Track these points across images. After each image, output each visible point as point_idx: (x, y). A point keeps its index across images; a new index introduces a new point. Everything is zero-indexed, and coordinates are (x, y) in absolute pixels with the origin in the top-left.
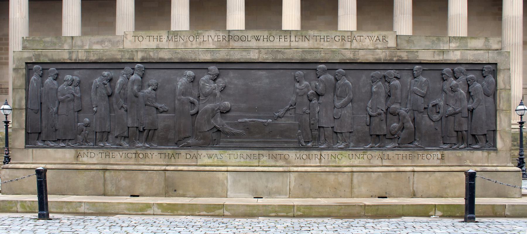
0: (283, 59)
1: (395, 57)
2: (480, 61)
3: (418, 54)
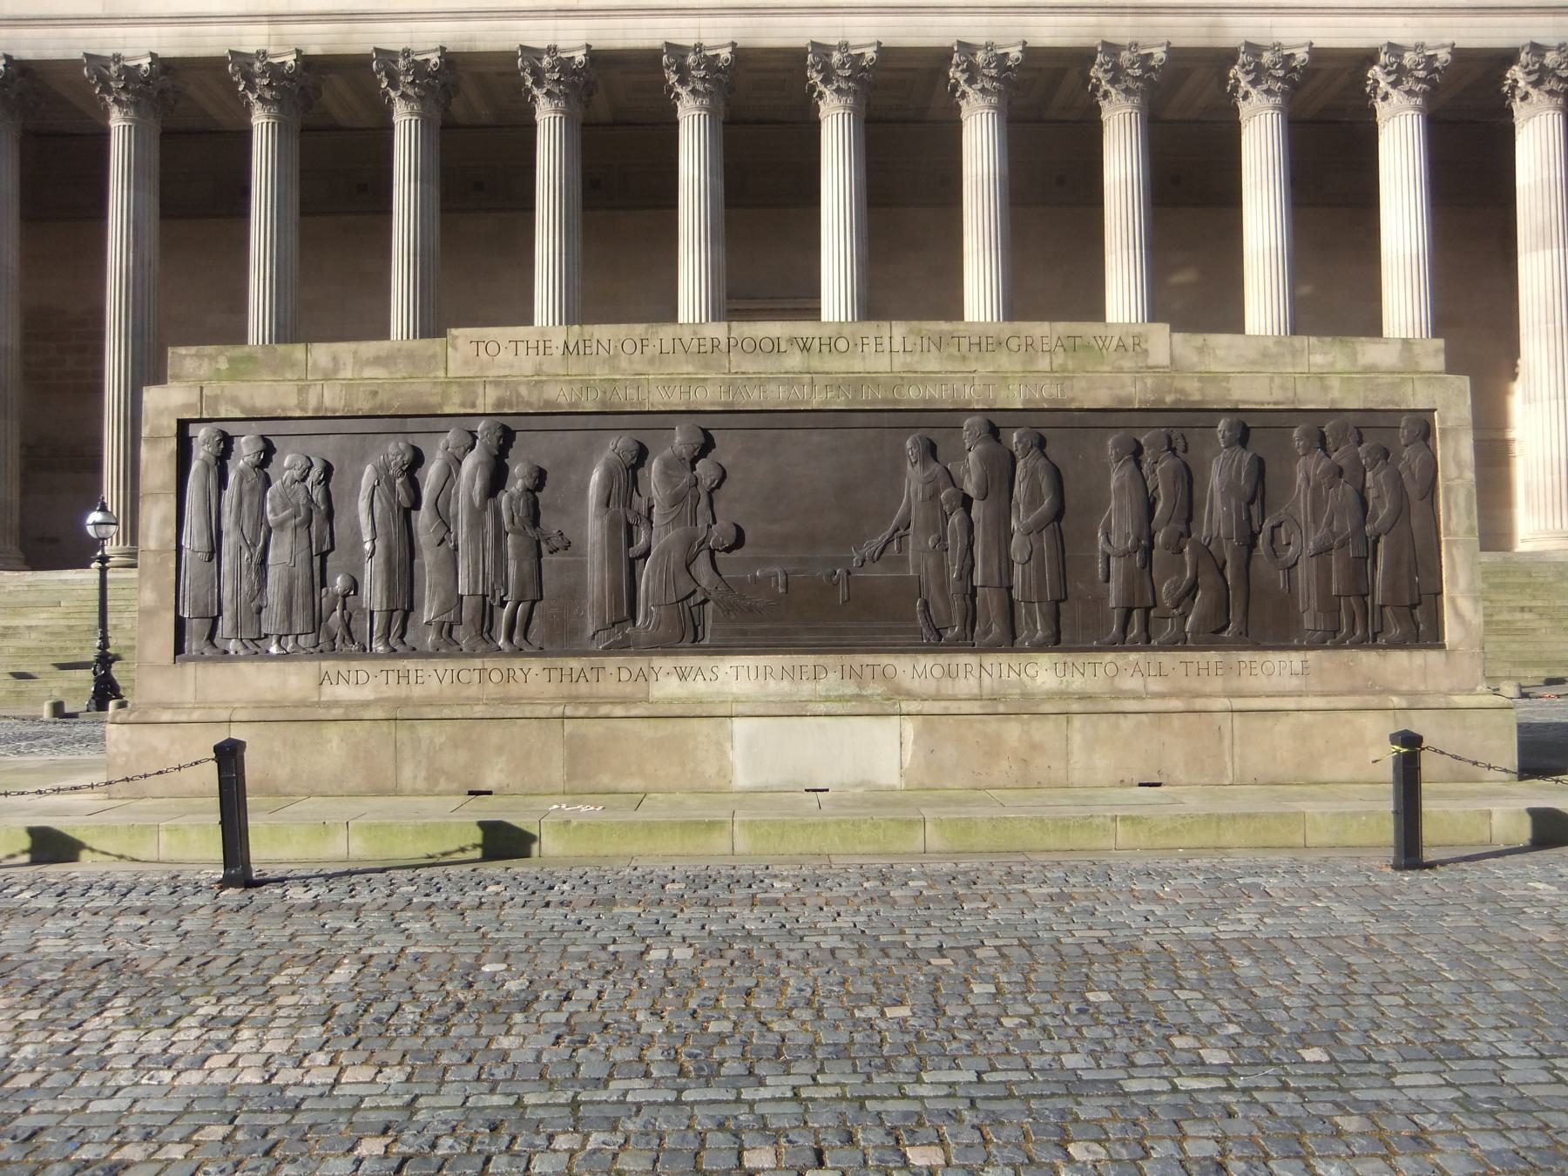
0: (875, 401)
1: (1169, 392)
2: (1393, 403)
3: (1229, 386)
